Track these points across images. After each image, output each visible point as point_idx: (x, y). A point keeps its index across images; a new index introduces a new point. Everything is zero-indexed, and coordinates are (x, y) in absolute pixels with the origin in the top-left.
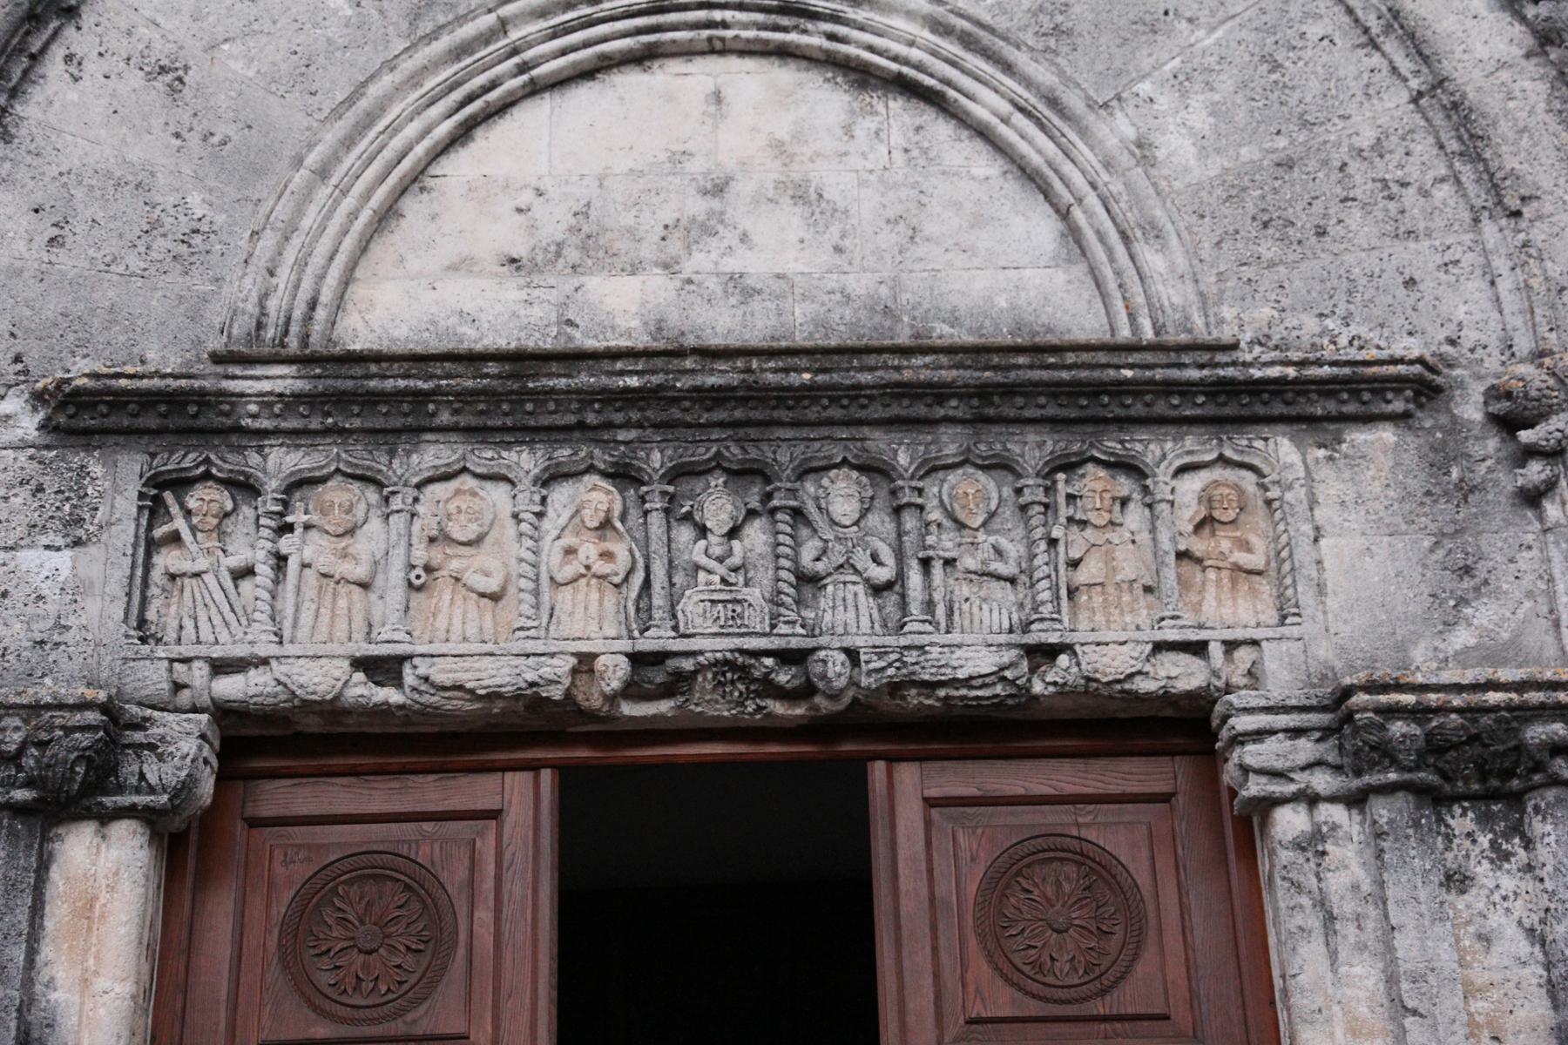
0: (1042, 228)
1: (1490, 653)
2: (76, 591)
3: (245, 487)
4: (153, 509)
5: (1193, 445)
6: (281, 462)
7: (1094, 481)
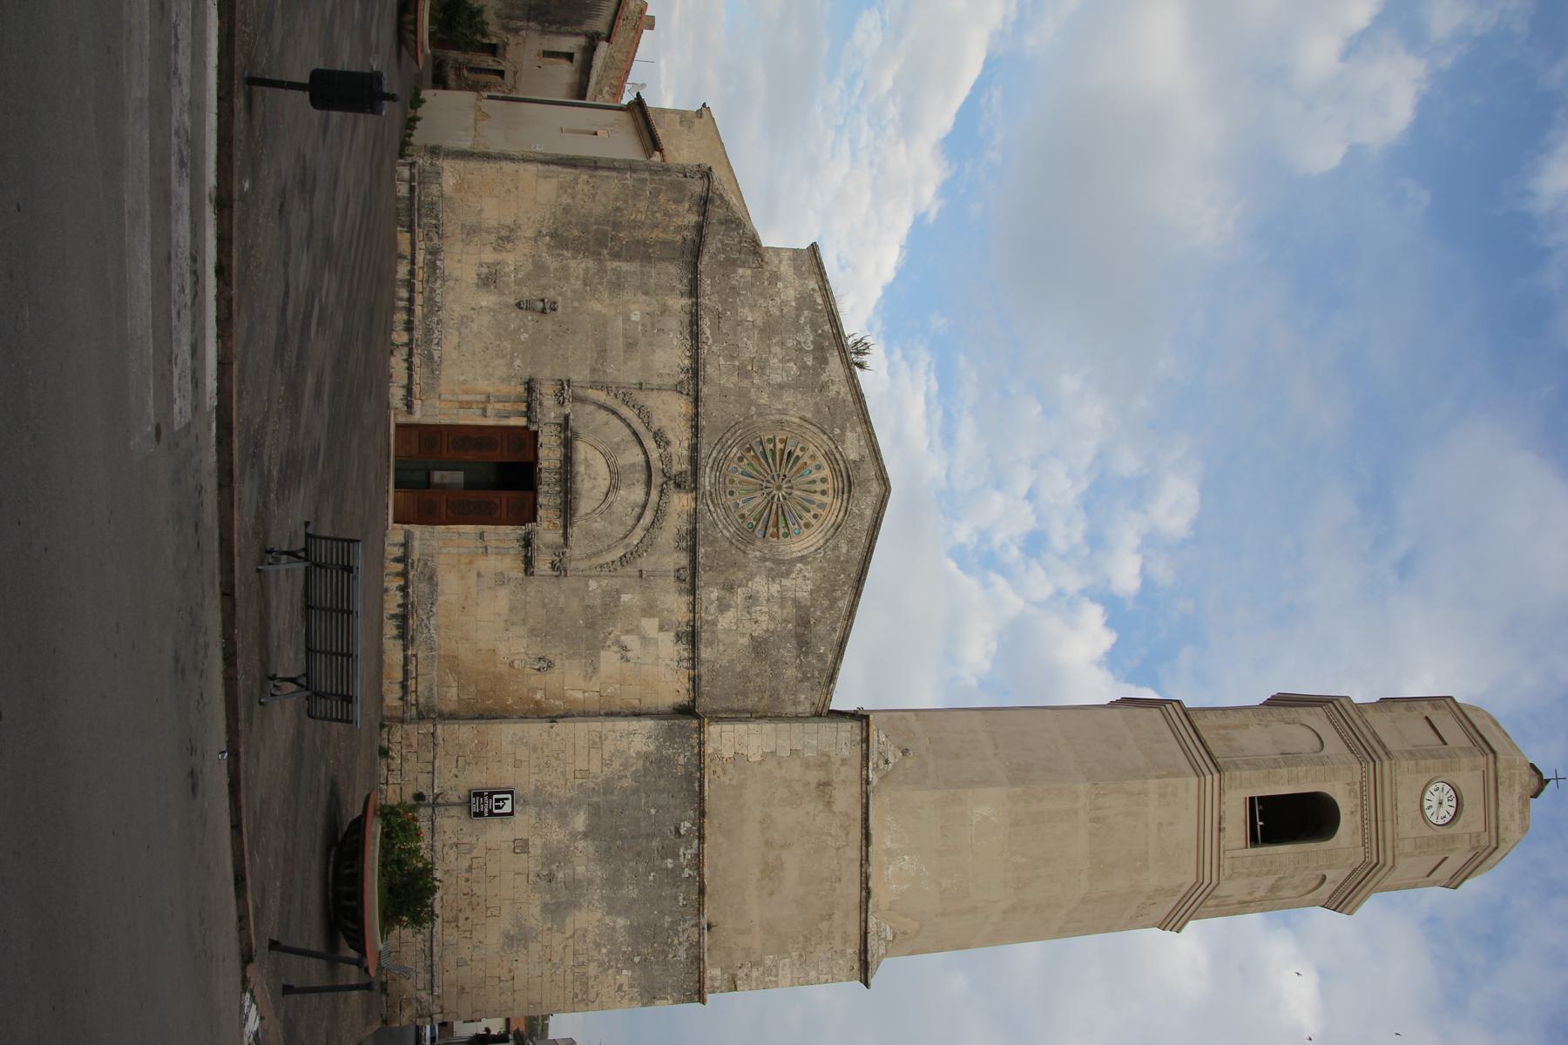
0: (589, 511)
1: (538, 547)
2: (550, 418)
3: (560, 432)
4: (558, 424)
5: (562, 521)
6: (562, 436)
7: (559, 513)
